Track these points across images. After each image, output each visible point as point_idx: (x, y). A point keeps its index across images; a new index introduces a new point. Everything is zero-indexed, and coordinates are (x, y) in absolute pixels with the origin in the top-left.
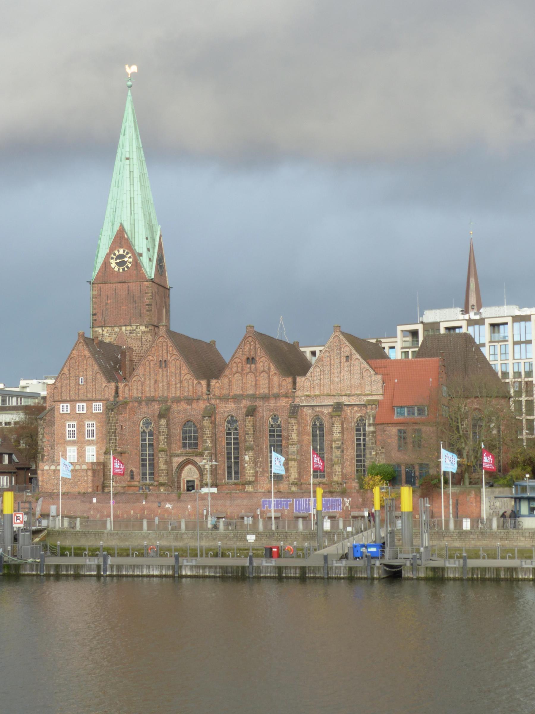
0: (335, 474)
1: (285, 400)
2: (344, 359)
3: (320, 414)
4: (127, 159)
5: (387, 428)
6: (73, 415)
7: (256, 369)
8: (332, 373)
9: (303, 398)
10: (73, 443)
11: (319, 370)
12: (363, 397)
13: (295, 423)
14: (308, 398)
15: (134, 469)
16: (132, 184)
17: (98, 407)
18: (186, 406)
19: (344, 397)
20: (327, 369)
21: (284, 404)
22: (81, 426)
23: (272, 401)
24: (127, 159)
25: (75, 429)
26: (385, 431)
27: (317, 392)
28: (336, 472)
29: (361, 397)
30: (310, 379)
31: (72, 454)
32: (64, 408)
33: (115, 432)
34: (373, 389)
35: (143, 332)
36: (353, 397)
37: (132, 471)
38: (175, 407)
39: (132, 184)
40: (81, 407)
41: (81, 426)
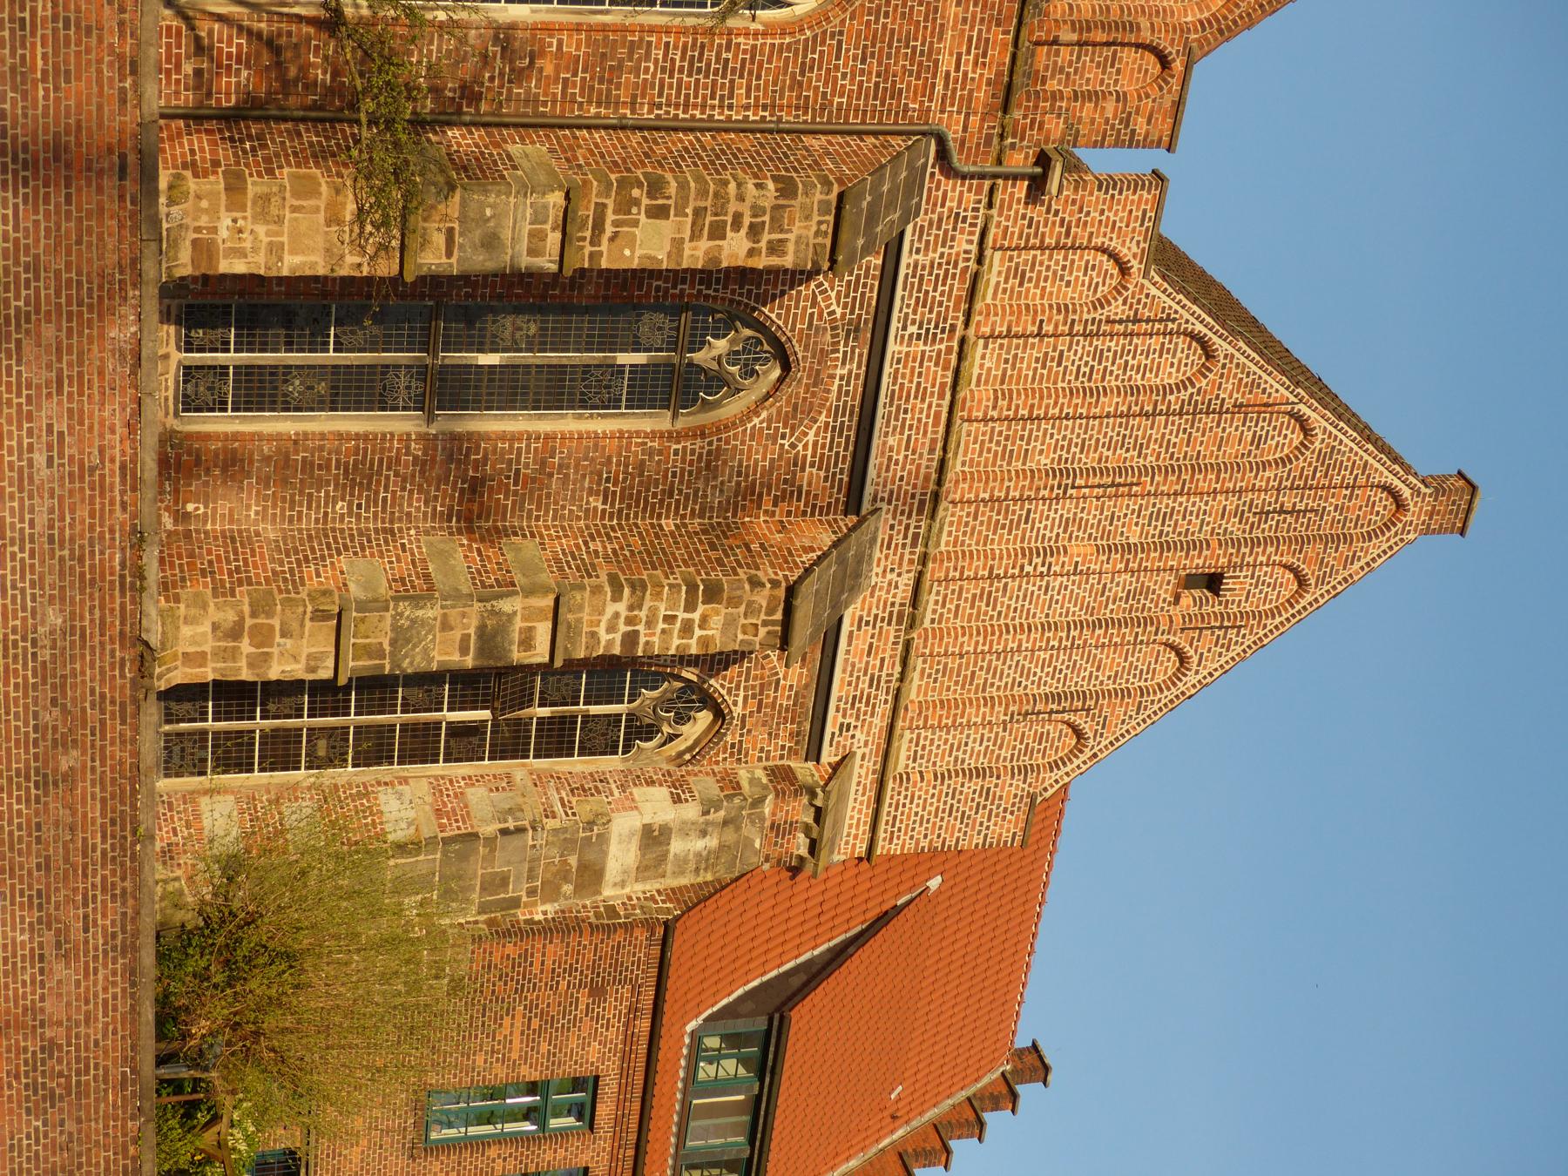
0: (235, 633)
1: (981, 80)
3: (797, 388)
5: (617, 1002)
8: (1118, 483)
9: (965, 243)
11: (1170, 376)
12: (879, 722)
13: (775, 248)
14: (959, 288)
19: (907, 580)
21: (946, 63)
26: (597, 992)
27: (982, 360)
28: (262, 637)
29: (883, 710)
30: (1117, 309)
34: (922, 790)
36: (890, 651)
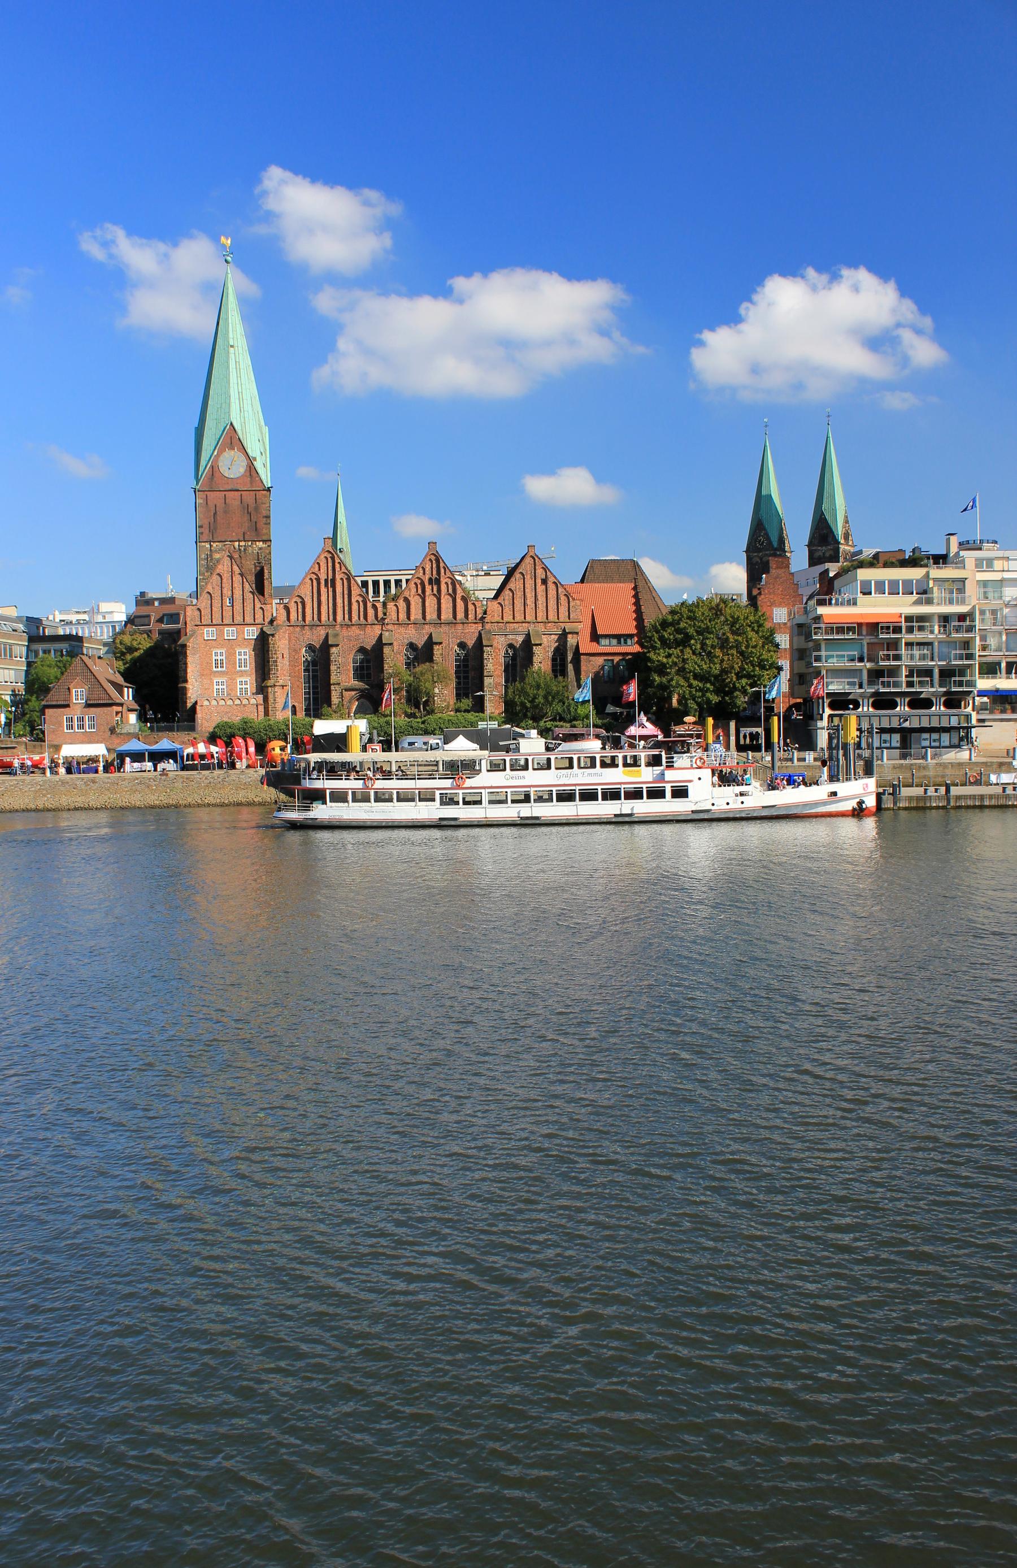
2: (539, 582)
3: (514, 642)
4: (232, 346)
6: (220, 642)
7: (439, 590)
10: (221, 674)
15: (296, 704)
16: (239, 377)
17: (252, 633)
18: (358, 631)
20: (519, 594)
22: (230, 655)
23: (460, 627)
24: (232, 346)
25: (224, 658)
31: (219, 684)
32: (209, 633)
33: (276, 661)
35: (260, 549)
37: (294, 707)
38: (345, 632)
39: (239, 377)
40: (230, 633)
41: (230, 655)
